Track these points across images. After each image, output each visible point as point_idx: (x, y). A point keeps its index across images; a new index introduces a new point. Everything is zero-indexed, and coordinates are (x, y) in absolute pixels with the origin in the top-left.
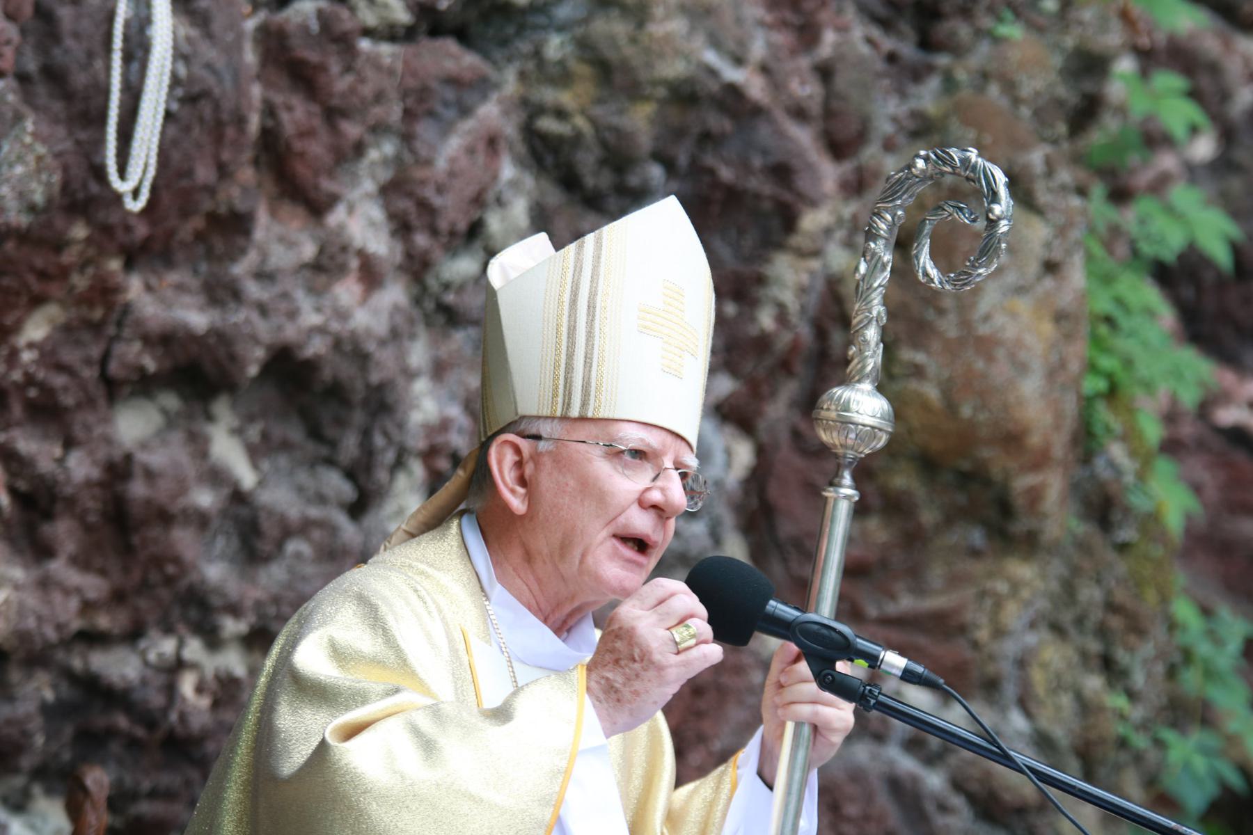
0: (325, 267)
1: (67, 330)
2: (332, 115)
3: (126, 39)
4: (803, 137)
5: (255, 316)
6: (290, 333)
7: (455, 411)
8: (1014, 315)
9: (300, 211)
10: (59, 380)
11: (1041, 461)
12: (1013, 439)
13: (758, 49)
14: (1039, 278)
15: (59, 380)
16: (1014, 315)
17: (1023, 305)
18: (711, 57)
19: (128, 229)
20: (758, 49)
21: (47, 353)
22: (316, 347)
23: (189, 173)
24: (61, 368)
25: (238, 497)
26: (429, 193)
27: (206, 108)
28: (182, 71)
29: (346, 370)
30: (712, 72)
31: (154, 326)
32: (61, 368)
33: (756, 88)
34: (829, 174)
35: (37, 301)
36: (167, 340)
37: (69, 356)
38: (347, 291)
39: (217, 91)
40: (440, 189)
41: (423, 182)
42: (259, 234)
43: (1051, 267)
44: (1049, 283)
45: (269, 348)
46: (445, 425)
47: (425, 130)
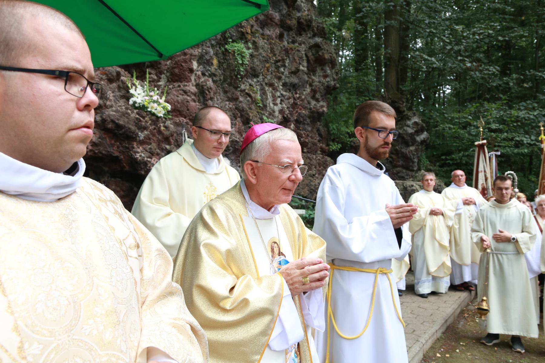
13: (238, 137)
20: (238, 137)
33: (238, 140)
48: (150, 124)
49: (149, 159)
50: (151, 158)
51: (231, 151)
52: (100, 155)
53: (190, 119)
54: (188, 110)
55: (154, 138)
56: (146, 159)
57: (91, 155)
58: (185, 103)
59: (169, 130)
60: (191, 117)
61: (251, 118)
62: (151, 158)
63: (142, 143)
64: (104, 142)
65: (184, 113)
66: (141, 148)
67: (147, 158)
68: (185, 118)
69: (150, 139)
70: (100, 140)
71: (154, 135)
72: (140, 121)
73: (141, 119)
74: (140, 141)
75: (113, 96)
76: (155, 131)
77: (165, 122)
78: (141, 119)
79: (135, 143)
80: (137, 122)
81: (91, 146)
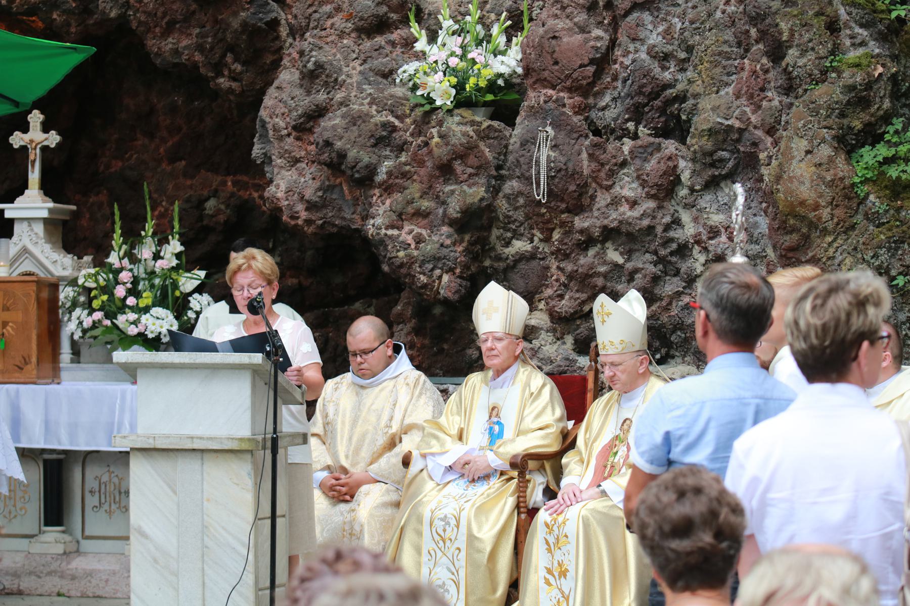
0: (615, 202)
1: (567, 233)
2: (602, 165)
3: (536, 161)
4: (759, 133)
5: (596, 220)
6: (606, 222)
7: (701, 230)
8: (800, 168)
9: (604, 191)
10: (564, 247)
11: (817, 207)
12: (802, 203)
14: (805, 156)
15: (564, 247)
16: (800, 168)
17: (802, 165)
18: (719, 120)
19: (559, 207)
21: (561, 241)
22: (615, 224)
23: (567, 189)
24: (566, 244)
25: (616, 265)
26: (645, 177)
27: (563, 173)
28: (552, 165)
29: (630, 229)
30: (722, 124)
31: (578, 229)
32: (566, 244)
33: (737, 124)
34: (769, 140)
35: (553, 229)
36: (582, 232)
37: (566, 241)
38: (624, 208)
39: (564, 167)
40: (648, 175)
41: (642, 174)
42: (597, 200)
43: (808, 152)
44: (809, 156)
45: (600, 227)
46: (700, 234)
47: (638, 162)
48: (412, 135)
49: (390, 232)
50: (400, 228)
51: (730, 164)
52: (335, 230)
53: (570, 90)
54: (556, 63)
55: (422, 171)
56: (383, 231)
57: (315, 234)
58: (547, 44)
59: (447, 144)
60: (568, 83)
61: (785, 38)
62: (400, 228)
63: (388, 189)
64: (334, 196)
65: (546, 74)
66: (388, 202)
67: (386, 229)
68: (553, 87)
69: (405, 175)
70: (320, 193)
71: (421, 163)
72: (394, 129)
73: (397, 123)
74: (380, 185)
75: (360, 72)
76: (425, 149)
77: (440, 123)
78: (397, 123)
79: (377, 192)
80: (384, 133)
81: (307, 209)
